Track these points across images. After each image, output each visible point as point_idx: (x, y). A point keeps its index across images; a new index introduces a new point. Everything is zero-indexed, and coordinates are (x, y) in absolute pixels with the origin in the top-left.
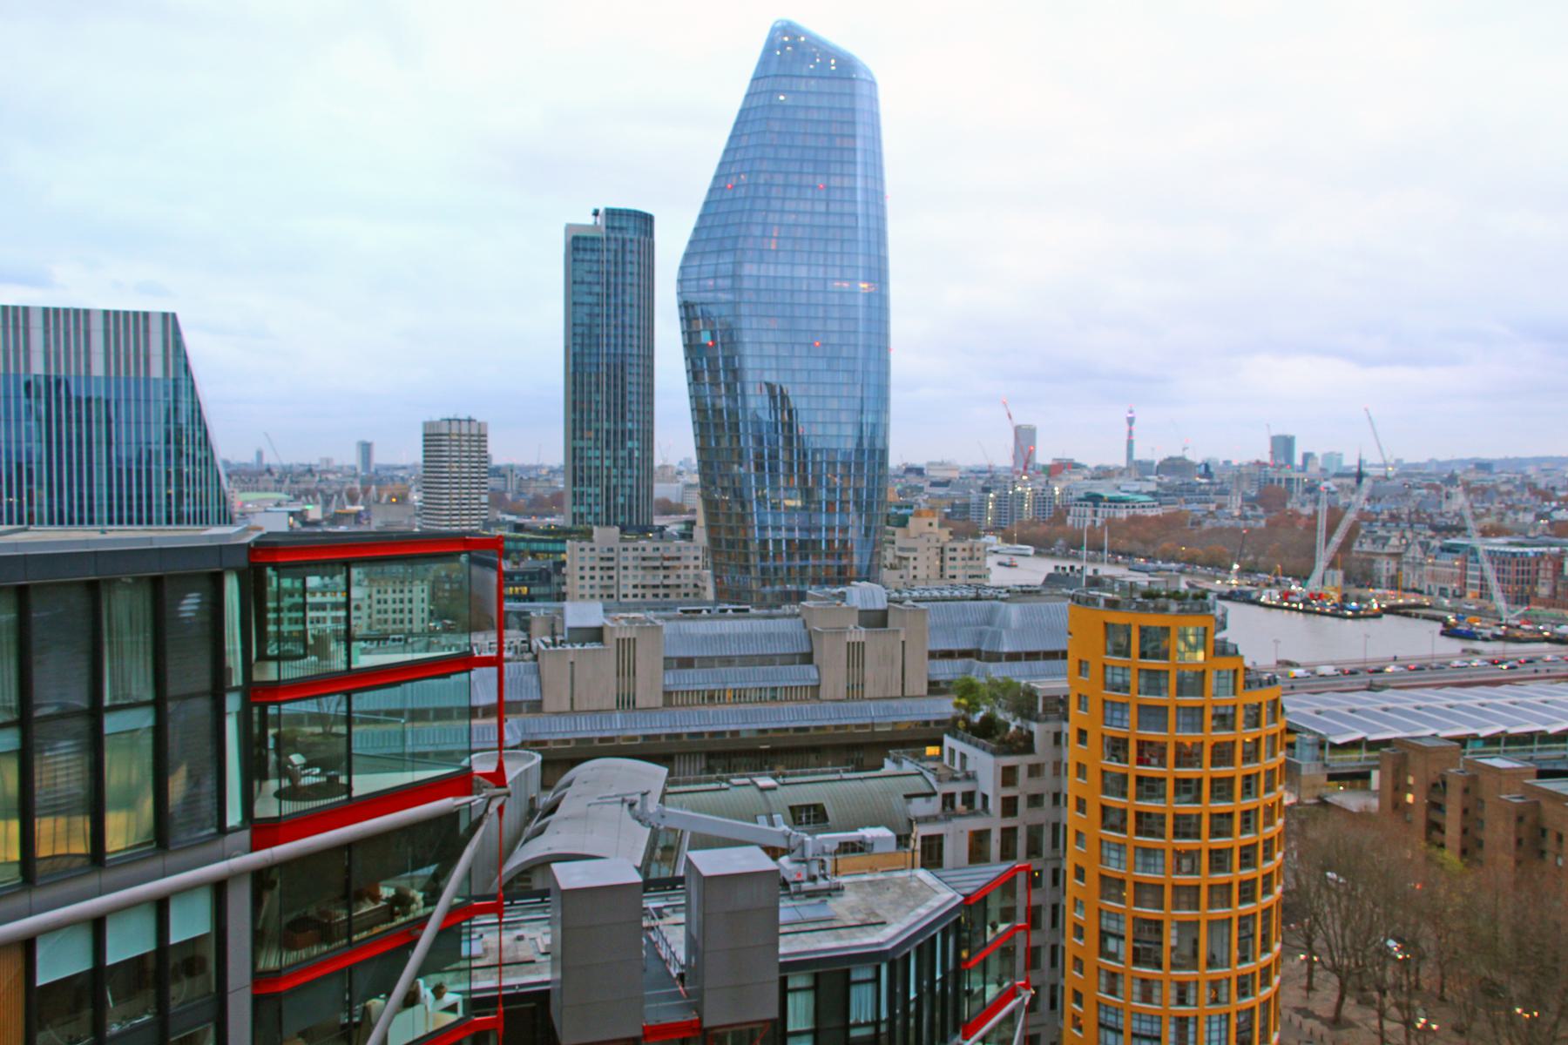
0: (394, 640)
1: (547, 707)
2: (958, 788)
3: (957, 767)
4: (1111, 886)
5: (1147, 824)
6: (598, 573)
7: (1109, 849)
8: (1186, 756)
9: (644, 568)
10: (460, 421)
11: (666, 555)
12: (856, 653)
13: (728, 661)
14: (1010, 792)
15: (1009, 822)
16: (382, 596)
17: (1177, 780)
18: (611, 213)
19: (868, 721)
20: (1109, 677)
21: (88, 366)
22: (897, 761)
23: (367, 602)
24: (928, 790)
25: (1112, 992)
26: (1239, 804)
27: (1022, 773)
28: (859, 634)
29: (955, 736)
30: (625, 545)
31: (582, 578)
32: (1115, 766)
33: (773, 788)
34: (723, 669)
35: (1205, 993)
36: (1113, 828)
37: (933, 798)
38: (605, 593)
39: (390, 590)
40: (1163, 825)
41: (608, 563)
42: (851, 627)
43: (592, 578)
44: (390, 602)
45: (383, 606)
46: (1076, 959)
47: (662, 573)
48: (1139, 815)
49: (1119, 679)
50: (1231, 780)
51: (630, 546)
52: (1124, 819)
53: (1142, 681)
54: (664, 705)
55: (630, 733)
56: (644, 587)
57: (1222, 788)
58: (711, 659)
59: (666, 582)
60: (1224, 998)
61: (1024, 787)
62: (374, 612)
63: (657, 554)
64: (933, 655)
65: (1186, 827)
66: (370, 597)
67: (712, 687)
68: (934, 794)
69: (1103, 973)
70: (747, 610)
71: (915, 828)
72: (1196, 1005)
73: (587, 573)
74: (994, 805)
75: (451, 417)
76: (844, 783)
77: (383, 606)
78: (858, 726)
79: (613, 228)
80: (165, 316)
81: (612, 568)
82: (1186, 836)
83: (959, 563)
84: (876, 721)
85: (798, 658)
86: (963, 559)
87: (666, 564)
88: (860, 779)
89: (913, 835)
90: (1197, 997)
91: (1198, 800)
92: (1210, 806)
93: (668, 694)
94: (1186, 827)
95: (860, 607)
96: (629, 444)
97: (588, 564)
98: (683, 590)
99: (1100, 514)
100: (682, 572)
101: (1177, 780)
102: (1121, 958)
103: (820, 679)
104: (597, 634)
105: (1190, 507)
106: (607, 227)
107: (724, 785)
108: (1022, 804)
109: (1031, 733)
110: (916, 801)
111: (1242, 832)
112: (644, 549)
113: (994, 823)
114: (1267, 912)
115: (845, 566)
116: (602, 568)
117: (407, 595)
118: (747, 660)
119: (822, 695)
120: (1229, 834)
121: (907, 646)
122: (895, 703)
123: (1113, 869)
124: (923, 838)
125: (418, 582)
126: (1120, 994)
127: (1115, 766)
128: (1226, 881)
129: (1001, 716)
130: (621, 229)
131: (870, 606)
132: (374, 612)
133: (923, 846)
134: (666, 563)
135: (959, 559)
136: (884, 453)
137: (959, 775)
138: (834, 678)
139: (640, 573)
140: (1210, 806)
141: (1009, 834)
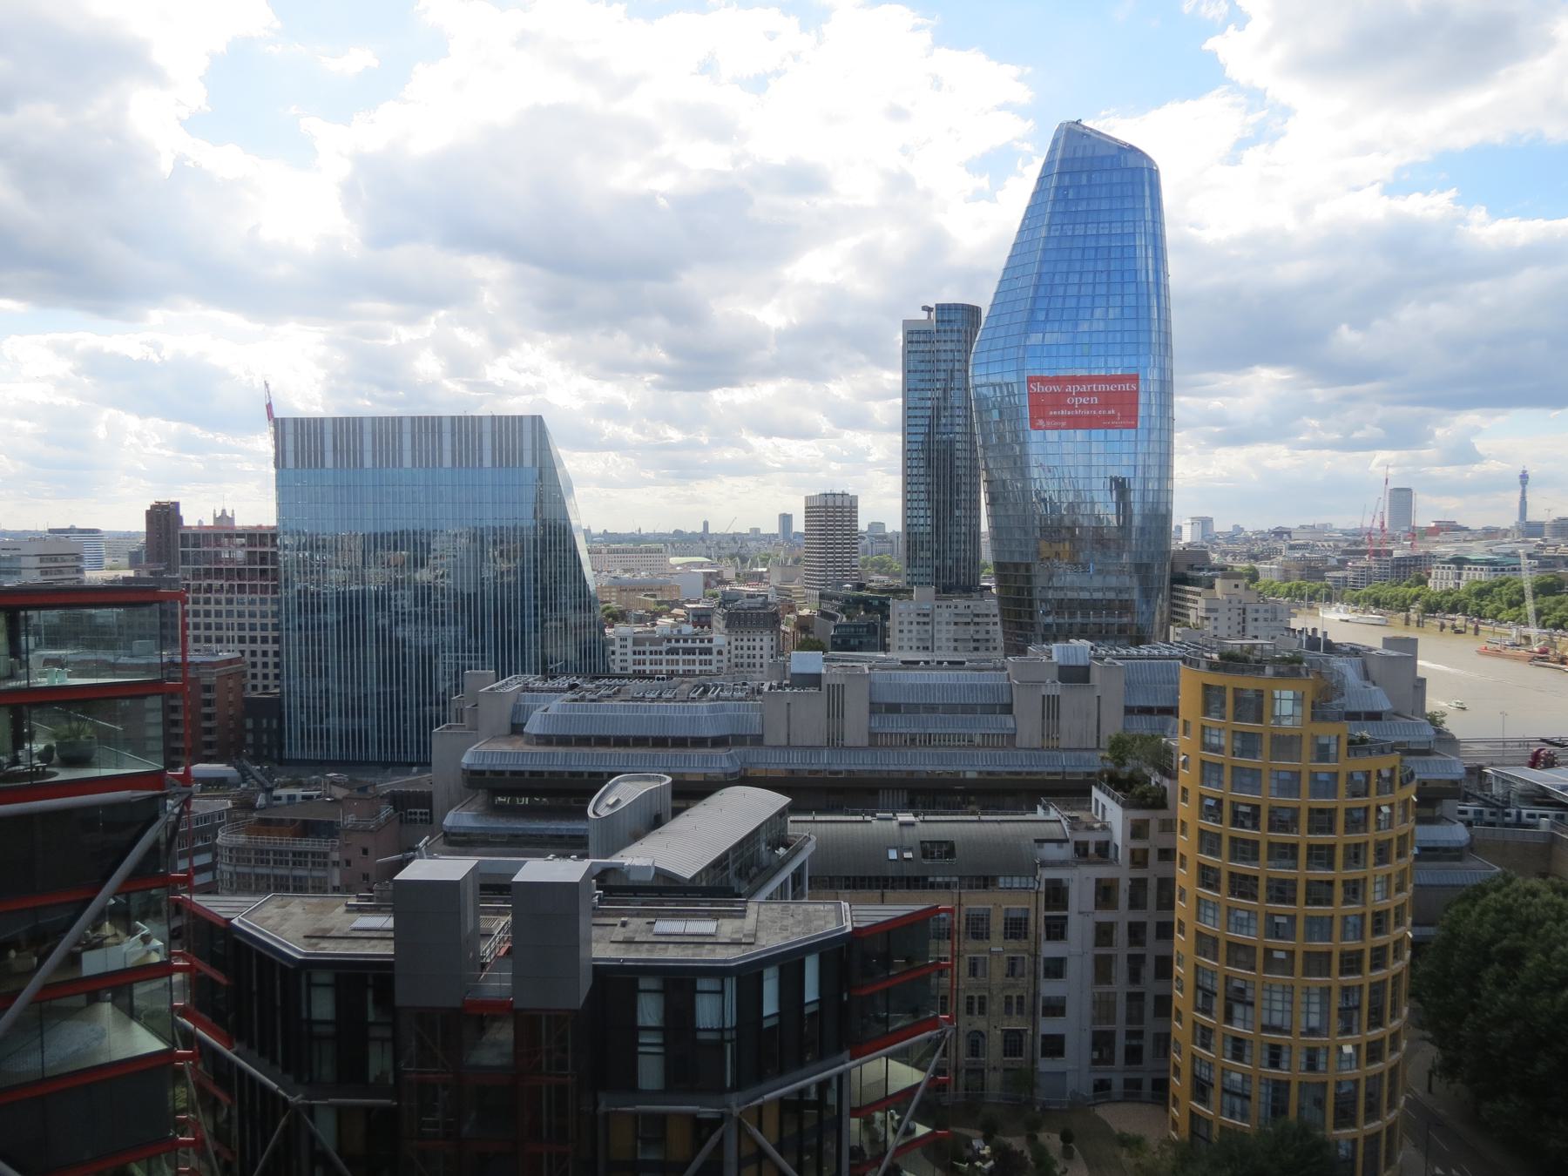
0: (658, 679)
1: (768, 740)
2: (1092, 838)
3: (1100, 818)
4: (1205, 943)
5: (1243, 886)
6: (914, 627)
7: (1206, 907)
8: (1282, 820)
9: (956, 624)
10: (834, 495)
11: (975, 612)
12: (1051, 707)
13: (931, 708)
14: (1139, 844)
15: (1139, 873)
16: (739, 643)
17: (1310, 847)
18: (941, 308)
19: (1060, 769)
20: (1207, 737)
21: (481, 459)
22: (1045, 808)
23: (728, 647)
24: (1063, 837)
25: (1206, 1046)
26: (1339, 874)
27: (1154, 827)
28: (1054, 688)
29: (1100, 789)
30: (939, 603)
31: (901, 631)
32: (1209, 825)
33: (911, 824)
34: (924, 715)
35: (1300, 1059)
36: (1209, 886)
37: (1065, 845)
38: (921, 645)
39: (745, 639)
40: (1295, 890)
41: (925, 618)
42: (1048, 681)
43: (910, 631)
44: (745, 648)
45: (740, 652)
46: (1178, 1012)
47: (972, 628)
48: (1232, 875)
49: (1215, 740)
50: (1332, 847)
51: (944, 604)
52: (1218, 880)
53: (1238, 744)
54: (870, 745)
55: (836, 768)
56: (956, 640)
57: (1322, 856)
58: (917, 705)
59: (976, 637)
60: (1321, 1067)
61: (1155, 840)
62: (733, 657)
63: (969, 611)
64: (1129, 711)
65: (1282, 891)
66: (729, 644)
67: (914, 731)
68: (1067, 841)
69: (1198, 1026)
70: (963, 663)
71: (1039, 871)
72: (1289, 1070)
73: (906, 627)
74: (1123, 856)
75: (828, 492)
76: (981, 825)
77: (740, 652)
78: (1049, 774)
79: (943, 321)
80: (533, 418)
81: (928, 623)
82: (1318, 902)
83: (1261, 623)
84: (1068, 770)
85: (998, 708)
86: (1266, 620)
87: (976, 619)
88: (996, 821)
89: (1037, 878)
90: (1290, 1062)
91: (1331, 866)
92: (1302, 873)
93: (873, 735)
94: (1282, 891)
95: (1062, 663)
96: (957, 513)
97: (906, 620)
98: (991, 645)
99: (1464, 577)
100: (991, 628)
101: (1310, 847)
102: (1214, 1014)
103: (1016, 729)
104: (814, 680)
105: (1201, 574)
106: (937, 321)
107: (868, 818)
108: (1153, 857)
109: (1165, 789)
110: (1047, 845)
111: (1346, 902)
112: (956, 607)
113: (1122, 872)
114: (1377, 988)
115: (1125, 625)
116: (918, 623)
117: (758, 644)
118: (951, 709)
119: (1018, 744)
120: (1329, 902)
121: (1102, 699)
122: (1086, 755)
123: (1208, 927)
124: (1048, 881)
125: (768, 632)
126: (1212, 1048)
127: (1209, 825)
128: (1325, 949)
129: (1147, 771)
130: (950, 321)
131: (1072, 662)
132: (733, 657)
133: (1047, 889)
134: (976, 620)
135: (1261, 619)
136: (1166, 518)
137: (1097, 825)
138: (1027, 725)
139: (952, 627)
140: (1302, 873)
141: (1138, 886)
